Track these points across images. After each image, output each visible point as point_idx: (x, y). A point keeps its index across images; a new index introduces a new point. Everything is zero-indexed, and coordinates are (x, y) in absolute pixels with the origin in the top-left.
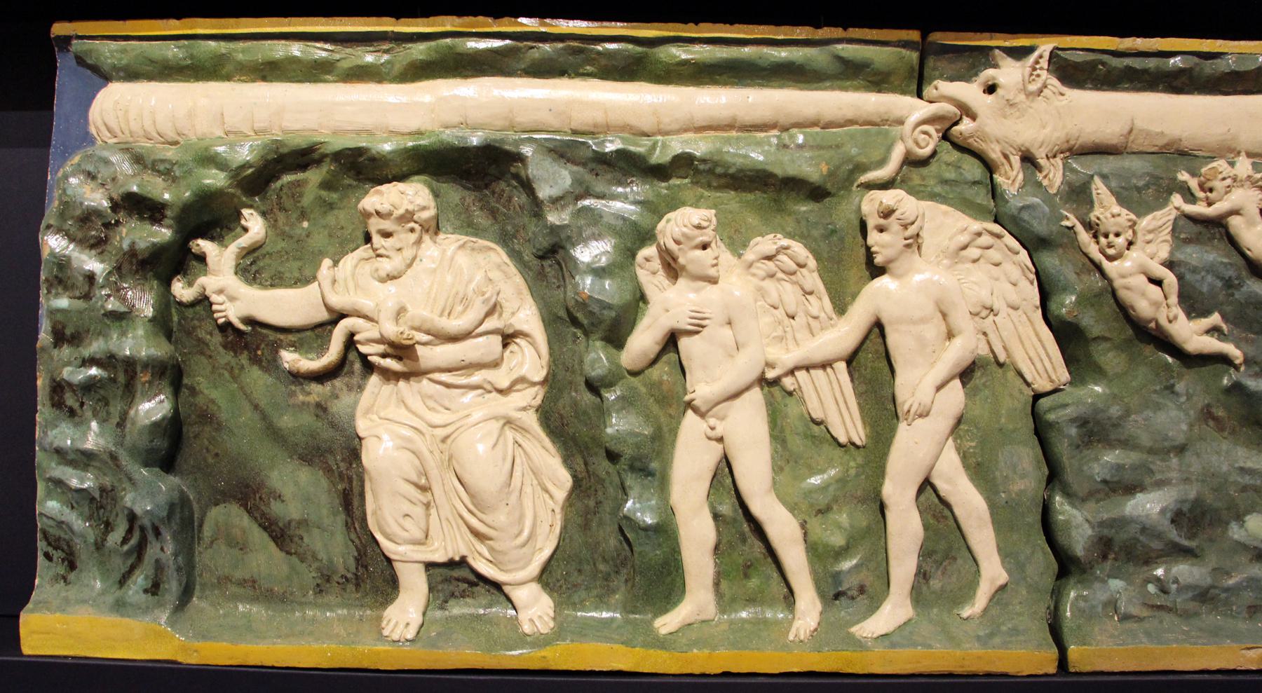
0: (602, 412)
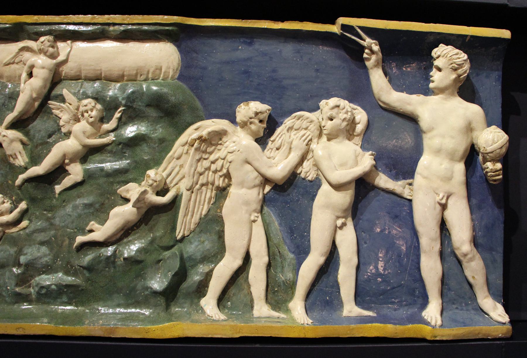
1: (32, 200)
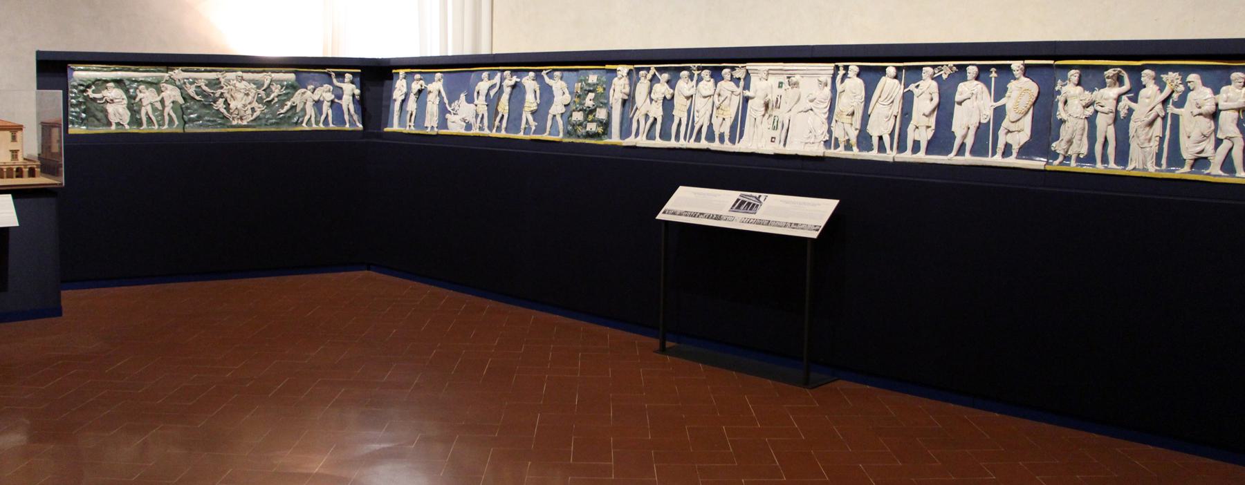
0: (133, 107)
1: (267, 105)
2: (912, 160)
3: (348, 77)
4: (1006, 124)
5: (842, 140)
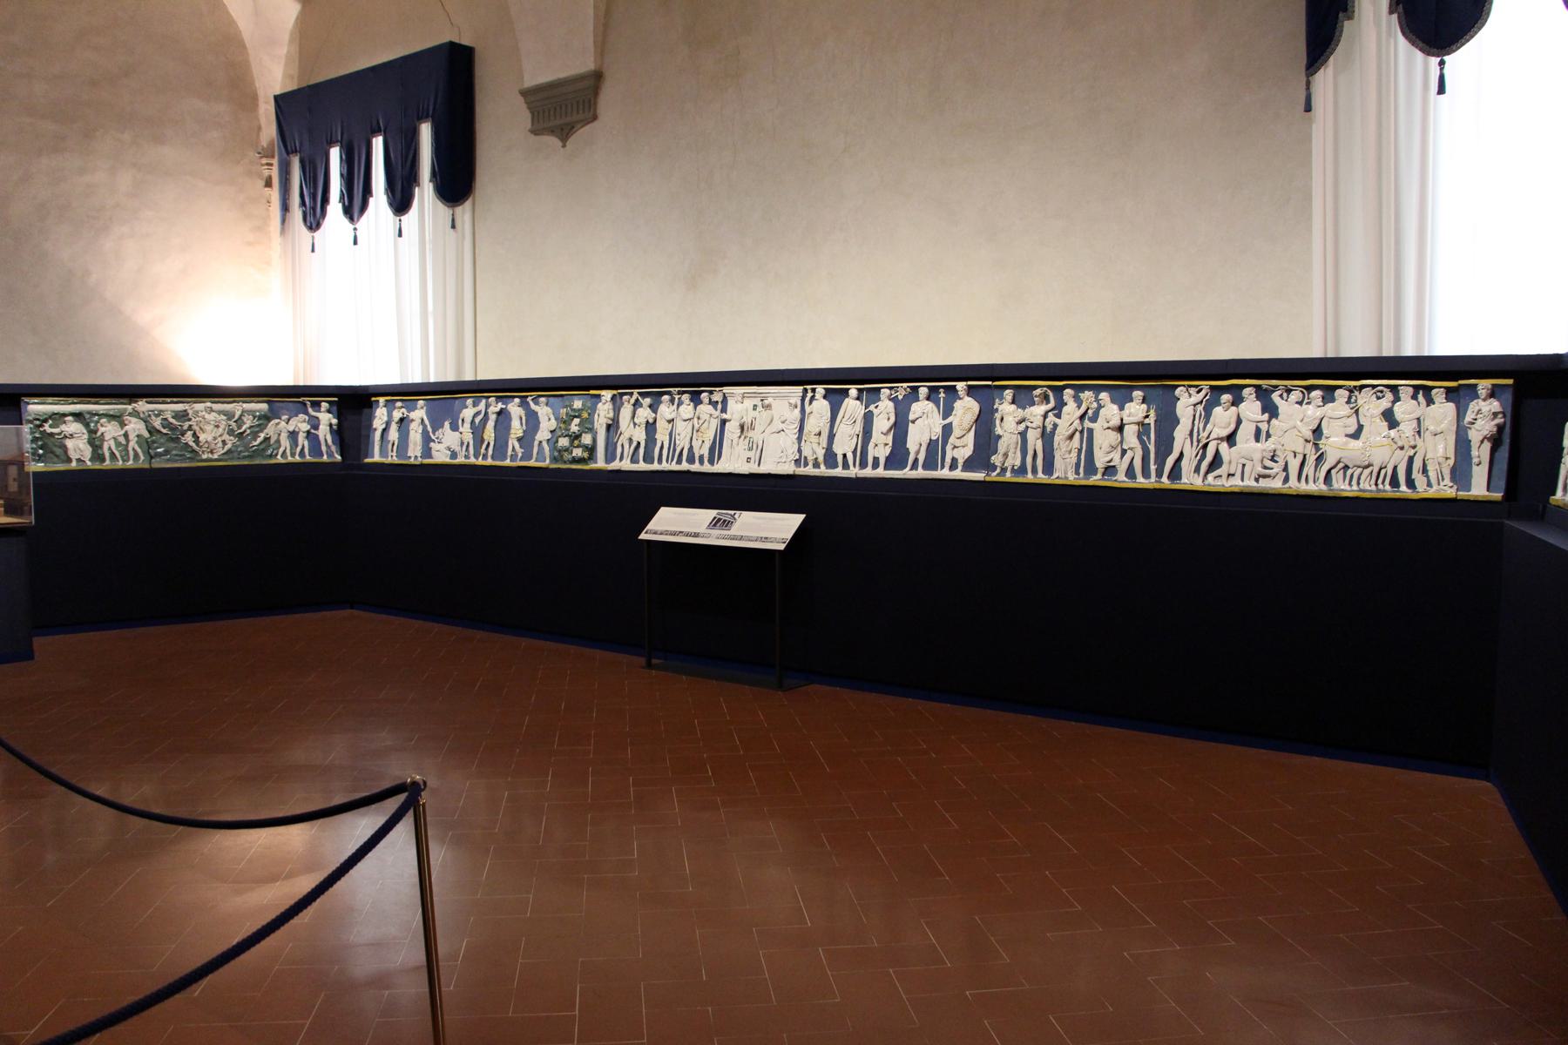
2: (872, 476)
3: (325, 406)
4: (952, 440)
5: (811, 458)
